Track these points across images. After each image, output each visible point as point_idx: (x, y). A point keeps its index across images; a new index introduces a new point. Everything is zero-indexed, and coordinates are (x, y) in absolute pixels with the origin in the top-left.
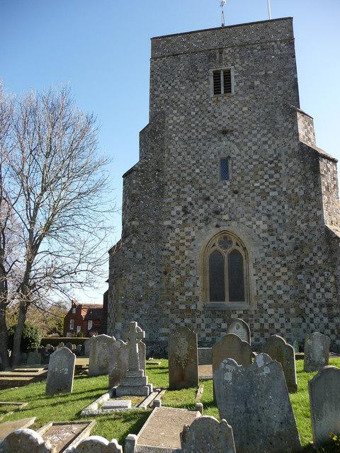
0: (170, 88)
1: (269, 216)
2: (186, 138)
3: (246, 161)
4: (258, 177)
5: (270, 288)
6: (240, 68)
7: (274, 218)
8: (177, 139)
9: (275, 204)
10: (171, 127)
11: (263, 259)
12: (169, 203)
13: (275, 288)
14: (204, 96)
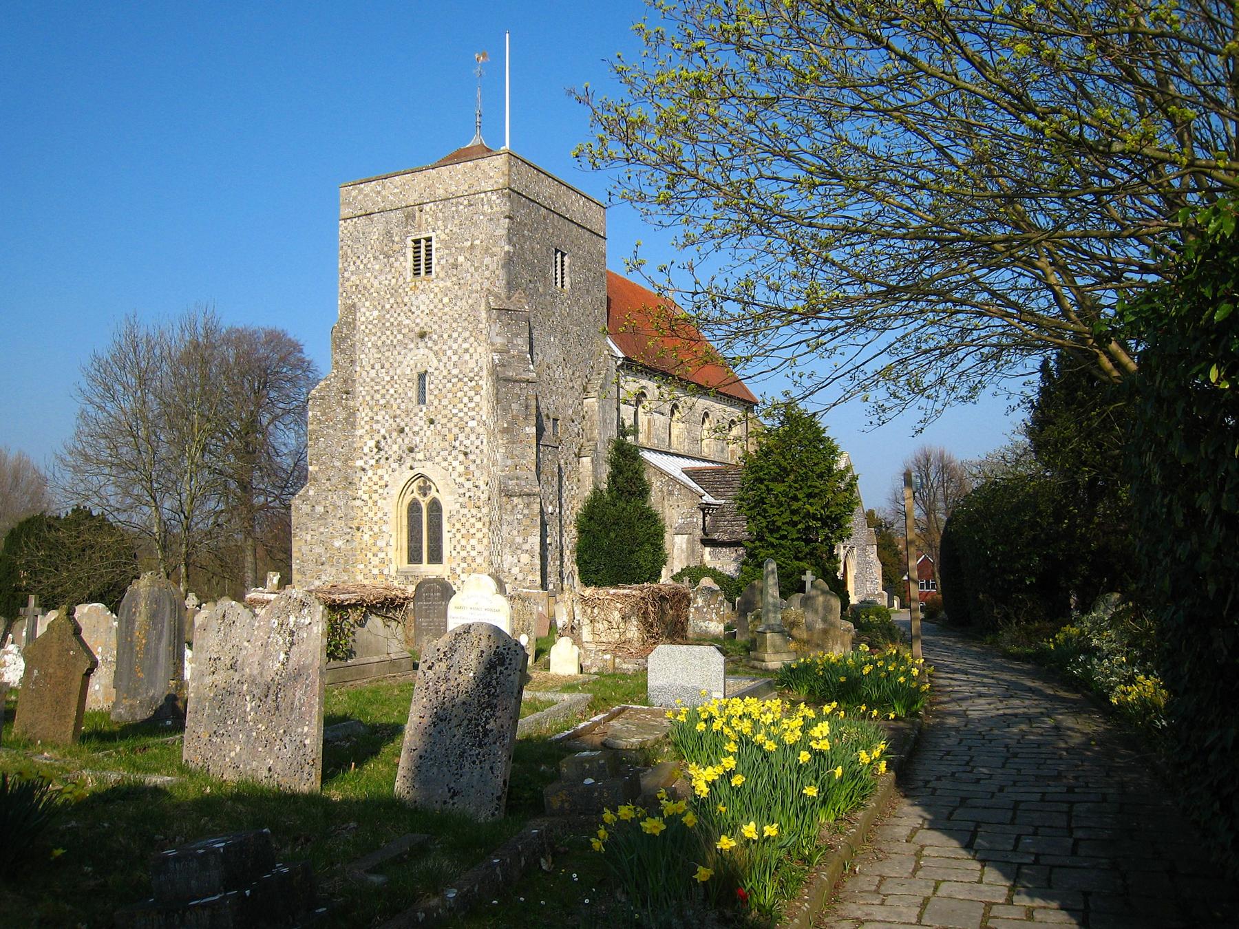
0: (362, 267)
1: (466, 454)
2: (379, 343)
3: (445, 377)
4: (457, 400)
5: (463, 548)
6: (443, 236)
7: (472, 457)
8: (370, 345)
9: (473, 437)
10: (363, 327)
11: (458, 512)
12: (361, 437)
13: (469, 548)
14: (401, 280)
